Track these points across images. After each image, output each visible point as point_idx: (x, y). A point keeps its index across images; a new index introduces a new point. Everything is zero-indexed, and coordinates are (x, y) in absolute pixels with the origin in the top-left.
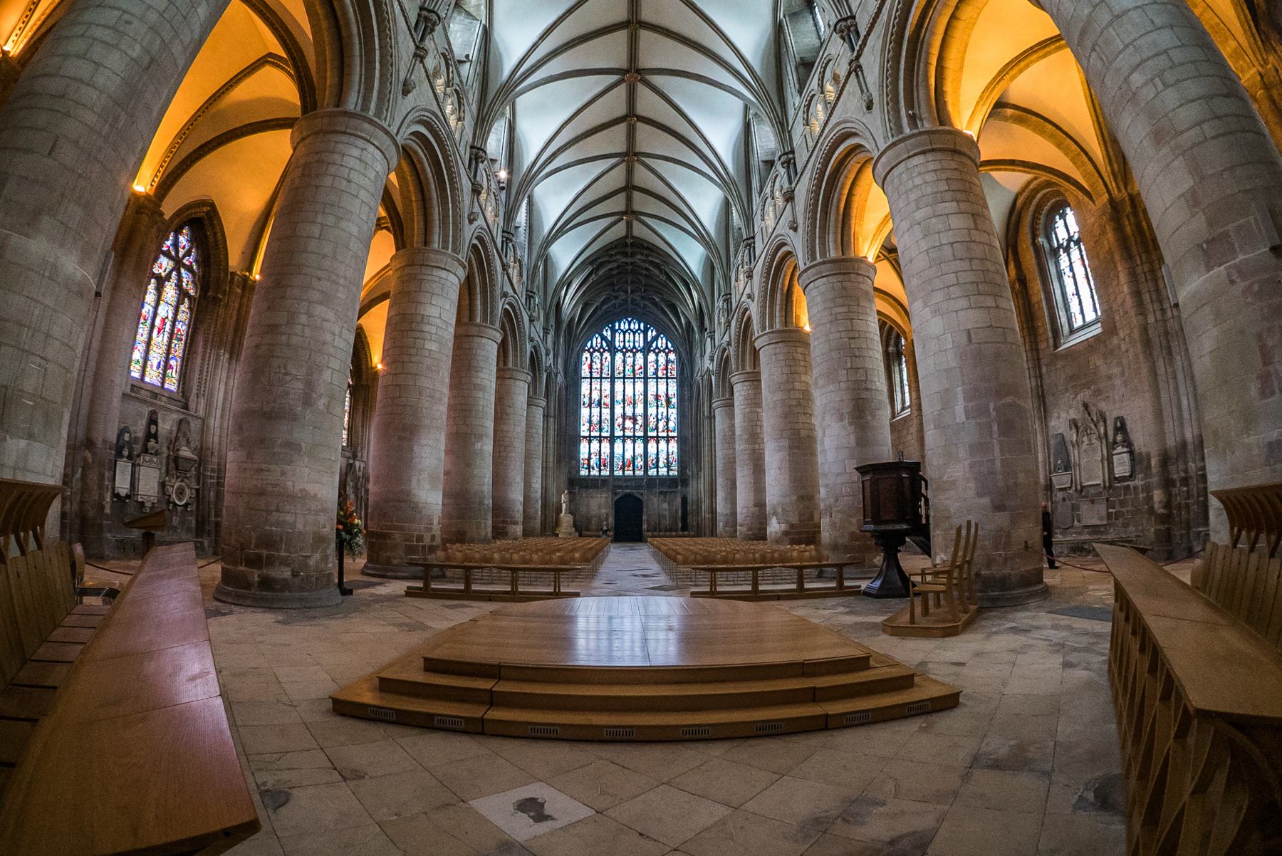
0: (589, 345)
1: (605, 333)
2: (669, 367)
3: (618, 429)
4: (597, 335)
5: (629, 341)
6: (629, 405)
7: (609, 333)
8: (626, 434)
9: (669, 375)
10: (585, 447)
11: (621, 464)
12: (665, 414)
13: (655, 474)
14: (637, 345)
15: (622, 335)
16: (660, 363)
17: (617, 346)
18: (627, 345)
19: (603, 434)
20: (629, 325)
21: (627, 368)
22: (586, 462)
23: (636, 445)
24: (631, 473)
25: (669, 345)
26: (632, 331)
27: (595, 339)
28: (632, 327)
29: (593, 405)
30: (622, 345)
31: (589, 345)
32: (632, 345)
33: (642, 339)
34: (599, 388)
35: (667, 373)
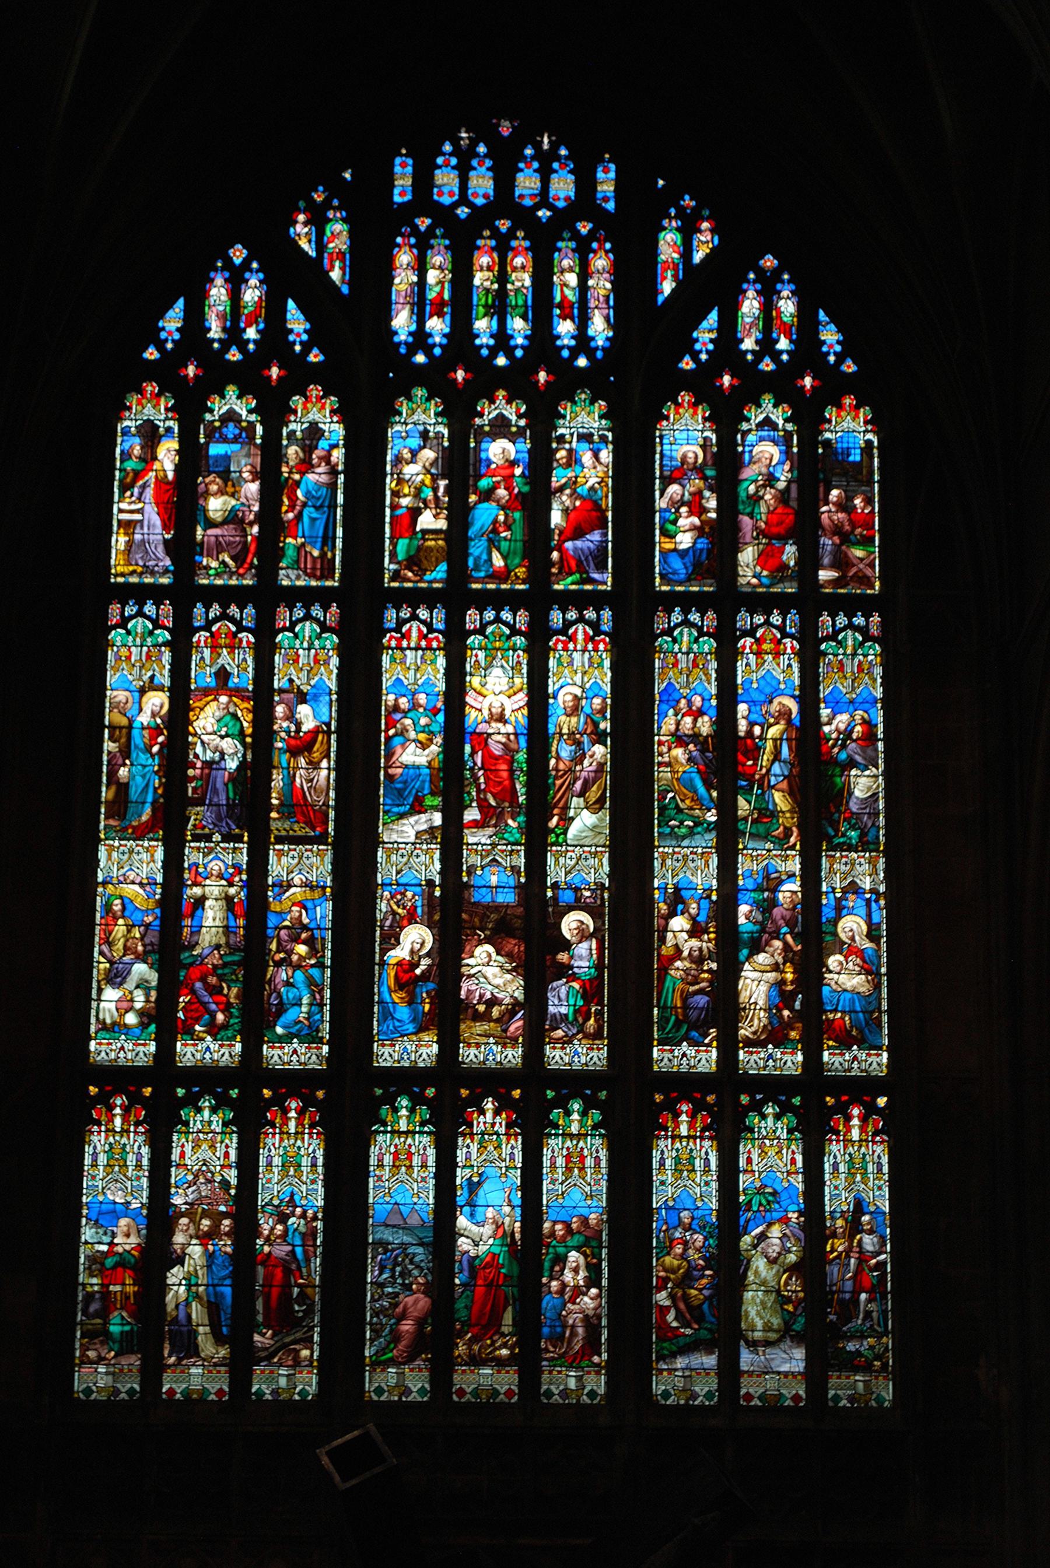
0: (172, 322)
1: (301, 231)
2: (828, 513)
3: (403, 1012)
4: (238, 254)
5: (499, 307)
6: (490, 816)
7: (338, 231)
8: (469, 1055)
9: (824, 575)
10: (117, 1159)
11: (417, 1302)
12: (790, 890)
13: (705, 1388)
14: (565, 328)
15: (438, 257)
16: (749, 484)
17: (402, 322)
18: (483, 326)
19: (276, 1056)
20: (504, 180)
21: (485, 514)
22: (126, 1287)
23: (554, 1149)
24: (506, 1381)
25: (830, 336)
26: (523, 217)
27: (218, 293)
28: (527, 182)
29: (196, 815)
30: (437, 326)
31: (172, 322)
32: (518, 326)
33: (601, 285)
34: (244, 677)
35: (809, 561)
